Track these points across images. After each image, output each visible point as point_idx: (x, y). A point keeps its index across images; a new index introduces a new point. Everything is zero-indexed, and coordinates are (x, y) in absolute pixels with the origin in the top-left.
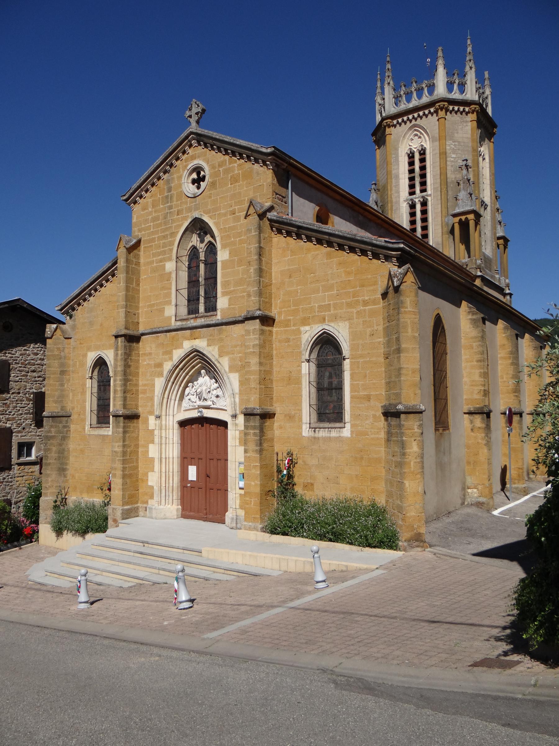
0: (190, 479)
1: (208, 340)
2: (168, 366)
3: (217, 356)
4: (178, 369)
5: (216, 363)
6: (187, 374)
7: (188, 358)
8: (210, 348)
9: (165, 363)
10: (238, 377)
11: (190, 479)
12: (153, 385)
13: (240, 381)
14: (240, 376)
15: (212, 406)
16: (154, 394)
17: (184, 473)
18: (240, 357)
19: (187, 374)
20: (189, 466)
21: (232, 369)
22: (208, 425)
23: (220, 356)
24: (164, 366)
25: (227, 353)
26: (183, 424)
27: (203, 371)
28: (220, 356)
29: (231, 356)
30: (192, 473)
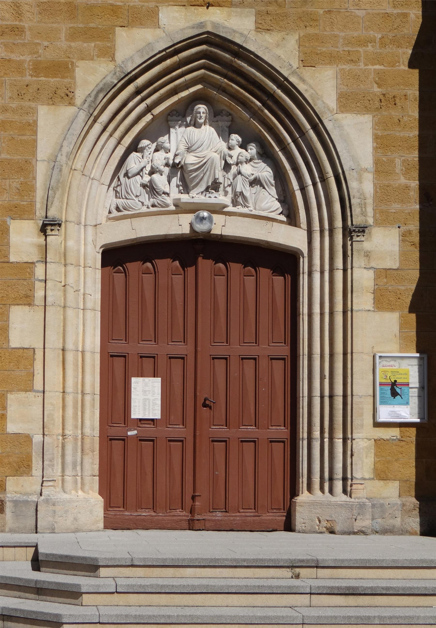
0: (137, 413)
1: (258, 14)
2: (91, 75)
3: (295, 64)
4: (131, 88)
5: (293, 79)
6: (149, 109)
7: (175, 59)
8: (269, 39)
9: (81, 64)
10: (370, 125)
11: (137, 413)
12: (32, 127)
13: (376, 138)
14: (376, 125)
15: (231, 209)
16: (34, 153)
17: (114, 399)
18: (378, 73)
19: (149, 109)
20: (134, 380)
21: (349, 101)
22: (209, 263)
23: (307, 61)
24: (79, 73)
25: (332, 59)
26: (114, 257)
27: (202, 108)
28: (307, 61)
29: (347, 67)
30: (146, 397)
